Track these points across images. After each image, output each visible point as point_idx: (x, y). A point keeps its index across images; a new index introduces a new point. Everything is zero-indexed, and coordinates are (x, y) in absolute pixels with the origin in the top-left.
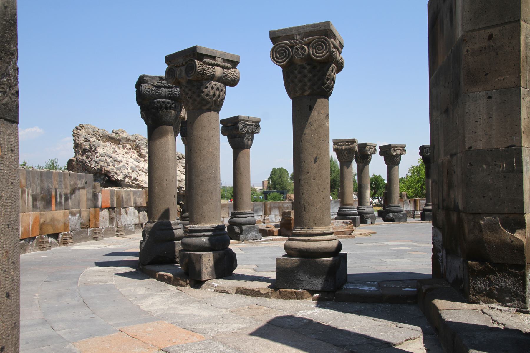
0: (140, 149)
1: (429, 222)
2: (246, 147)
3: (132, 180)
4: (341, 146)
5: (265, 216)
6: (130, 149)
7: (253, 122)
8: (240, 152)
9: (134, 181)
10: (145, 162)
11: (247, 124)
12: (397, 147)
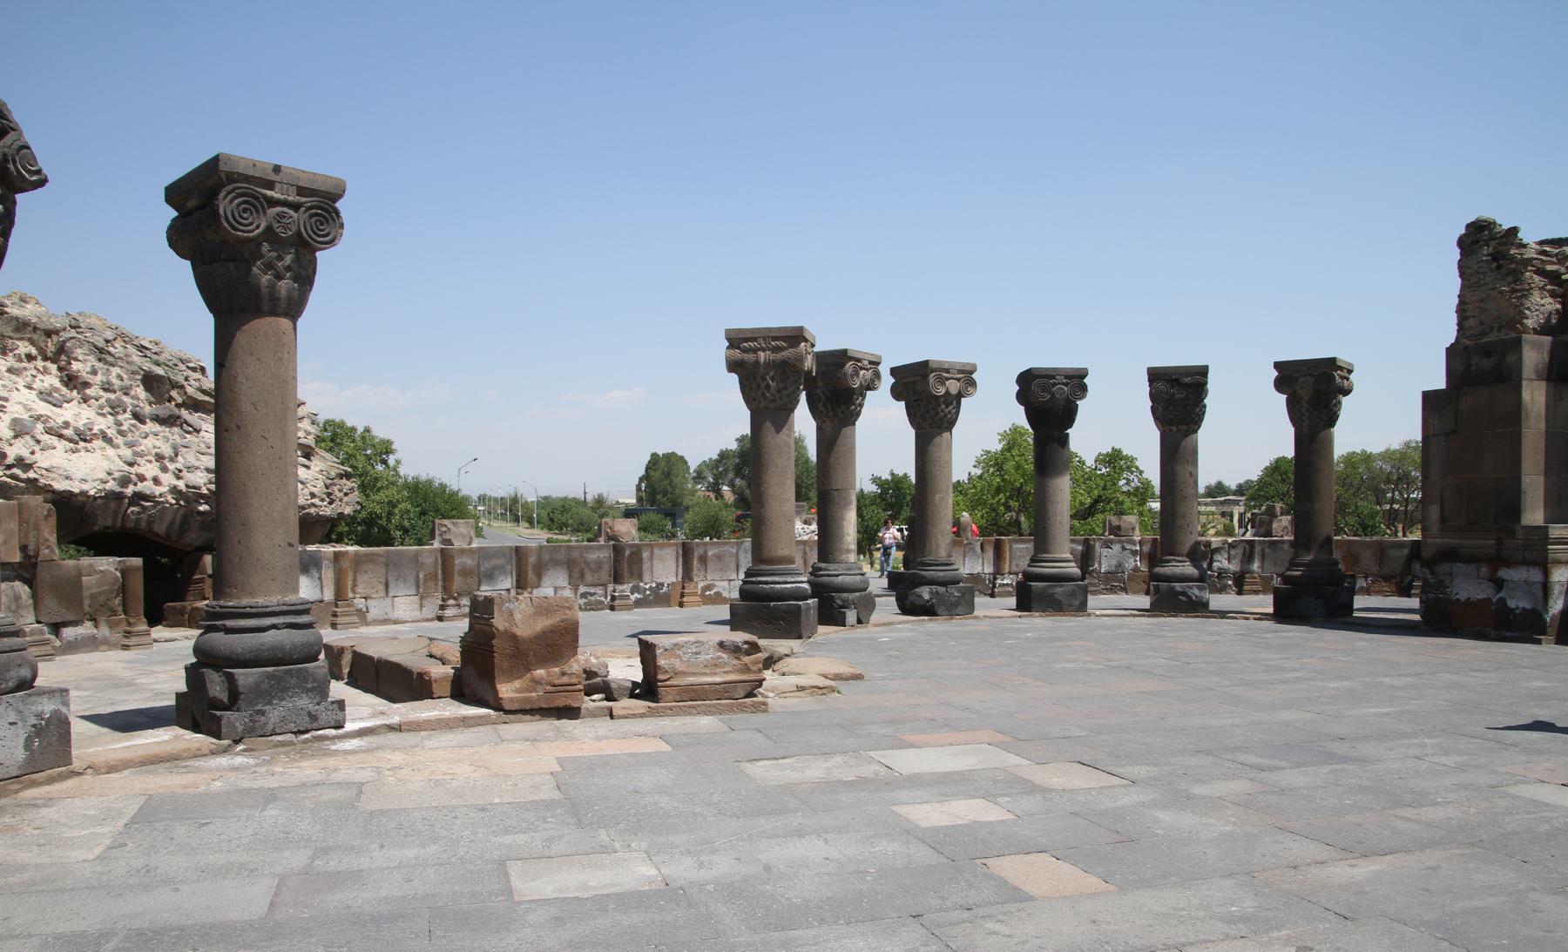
0: (70, 359)
1: (1041, 616)
2: (266, 307)
3: (9, 467)
4: (755, 351)
5: (520, 591)
6: (30, 358)
7: (302, 191)
8: (238, 328)
9: (15, 471)
10: (84, 406)
11: (264, 196)
12: (947, 371)
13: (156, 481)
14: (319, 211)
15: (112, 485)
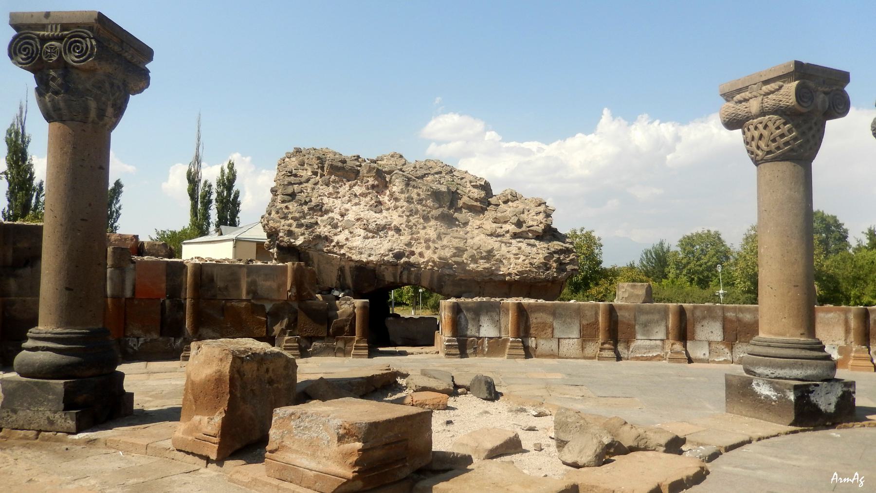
4: (746, 100)
7: (65, 27)
11: (38, 35)
13: (421, 255)
14: (77, 39)
15: (389, 258)
